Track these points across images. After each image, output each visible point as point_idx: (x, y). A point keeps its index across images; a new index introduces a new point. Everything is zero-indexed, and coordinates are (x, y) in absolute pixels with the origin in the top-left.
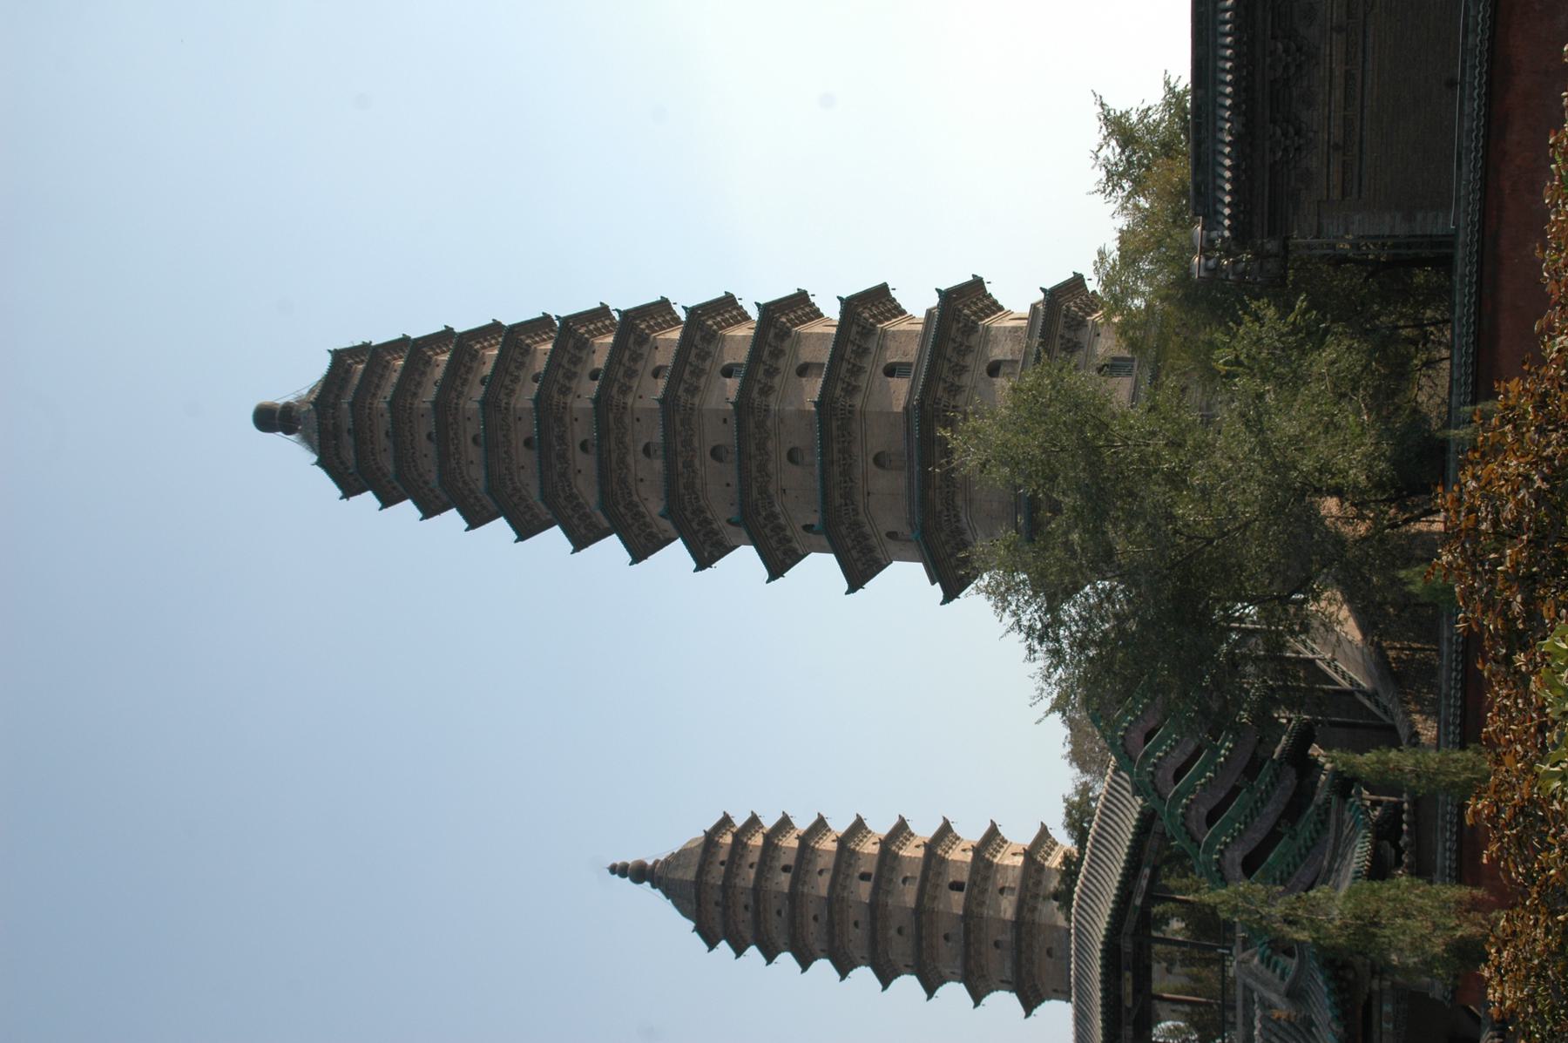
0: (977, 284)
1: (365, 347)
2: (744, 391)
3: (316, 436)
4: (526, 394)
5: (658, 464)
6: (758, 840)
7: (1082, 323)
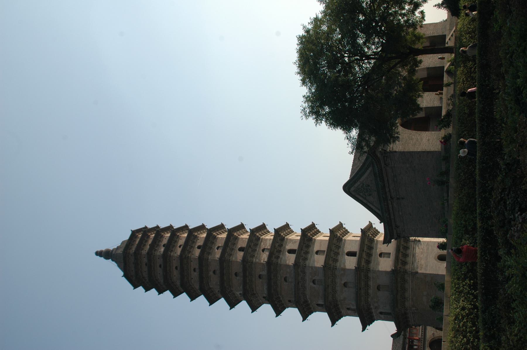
2: (270, 257)
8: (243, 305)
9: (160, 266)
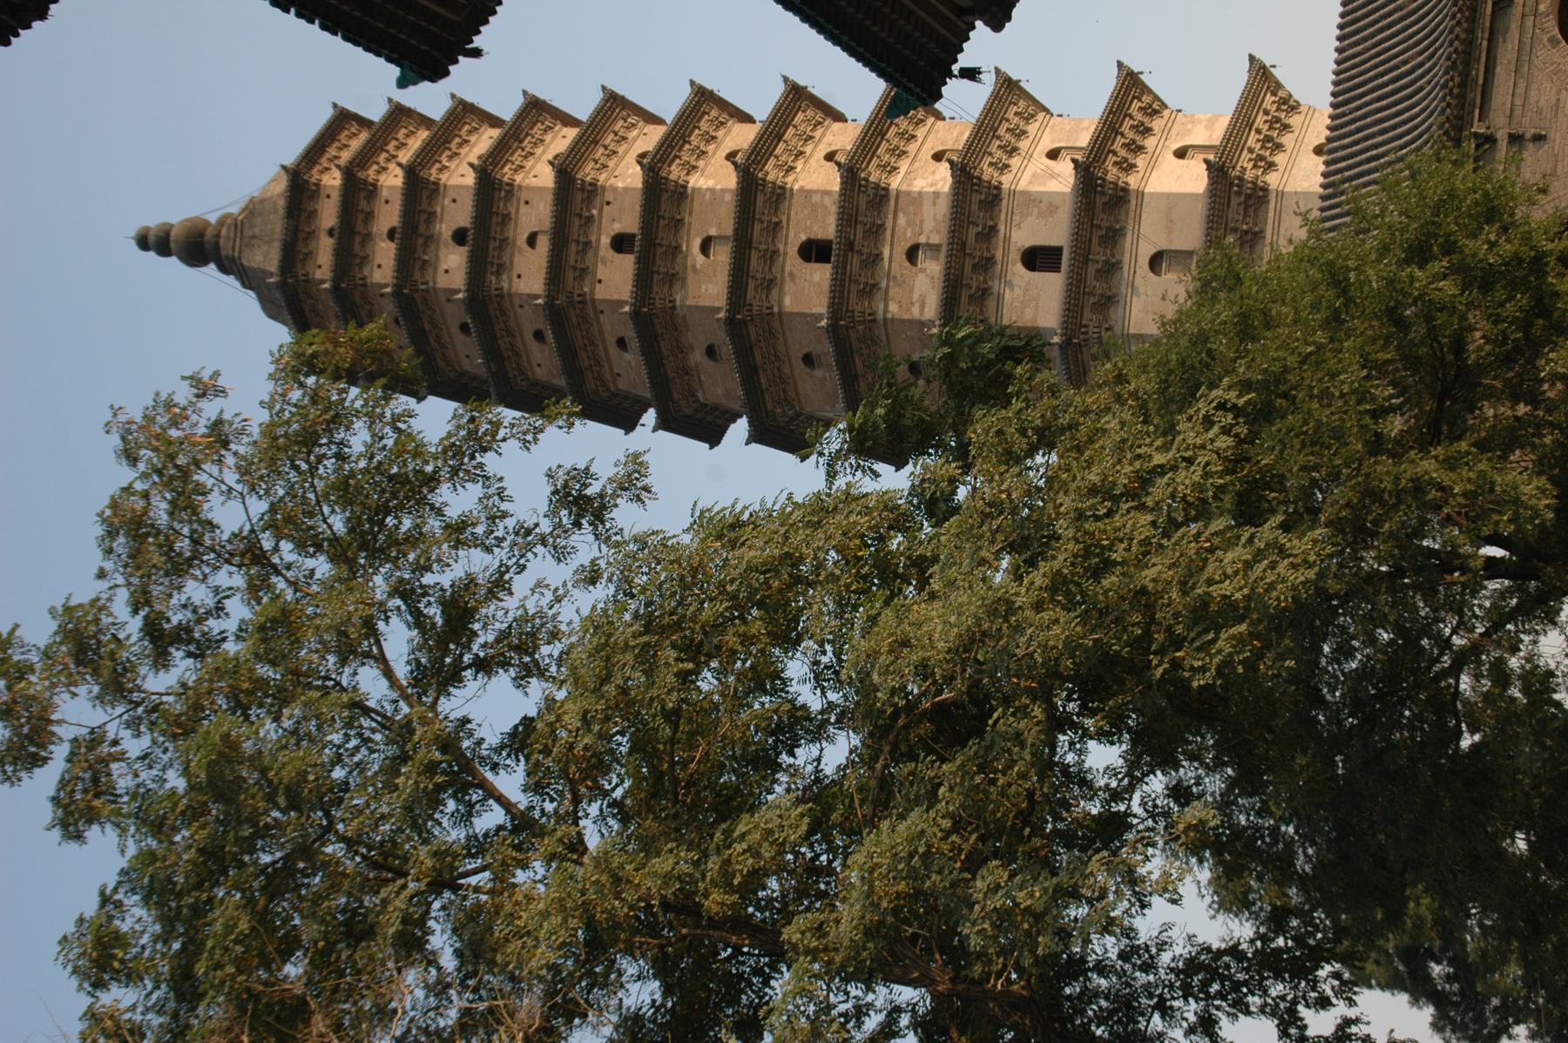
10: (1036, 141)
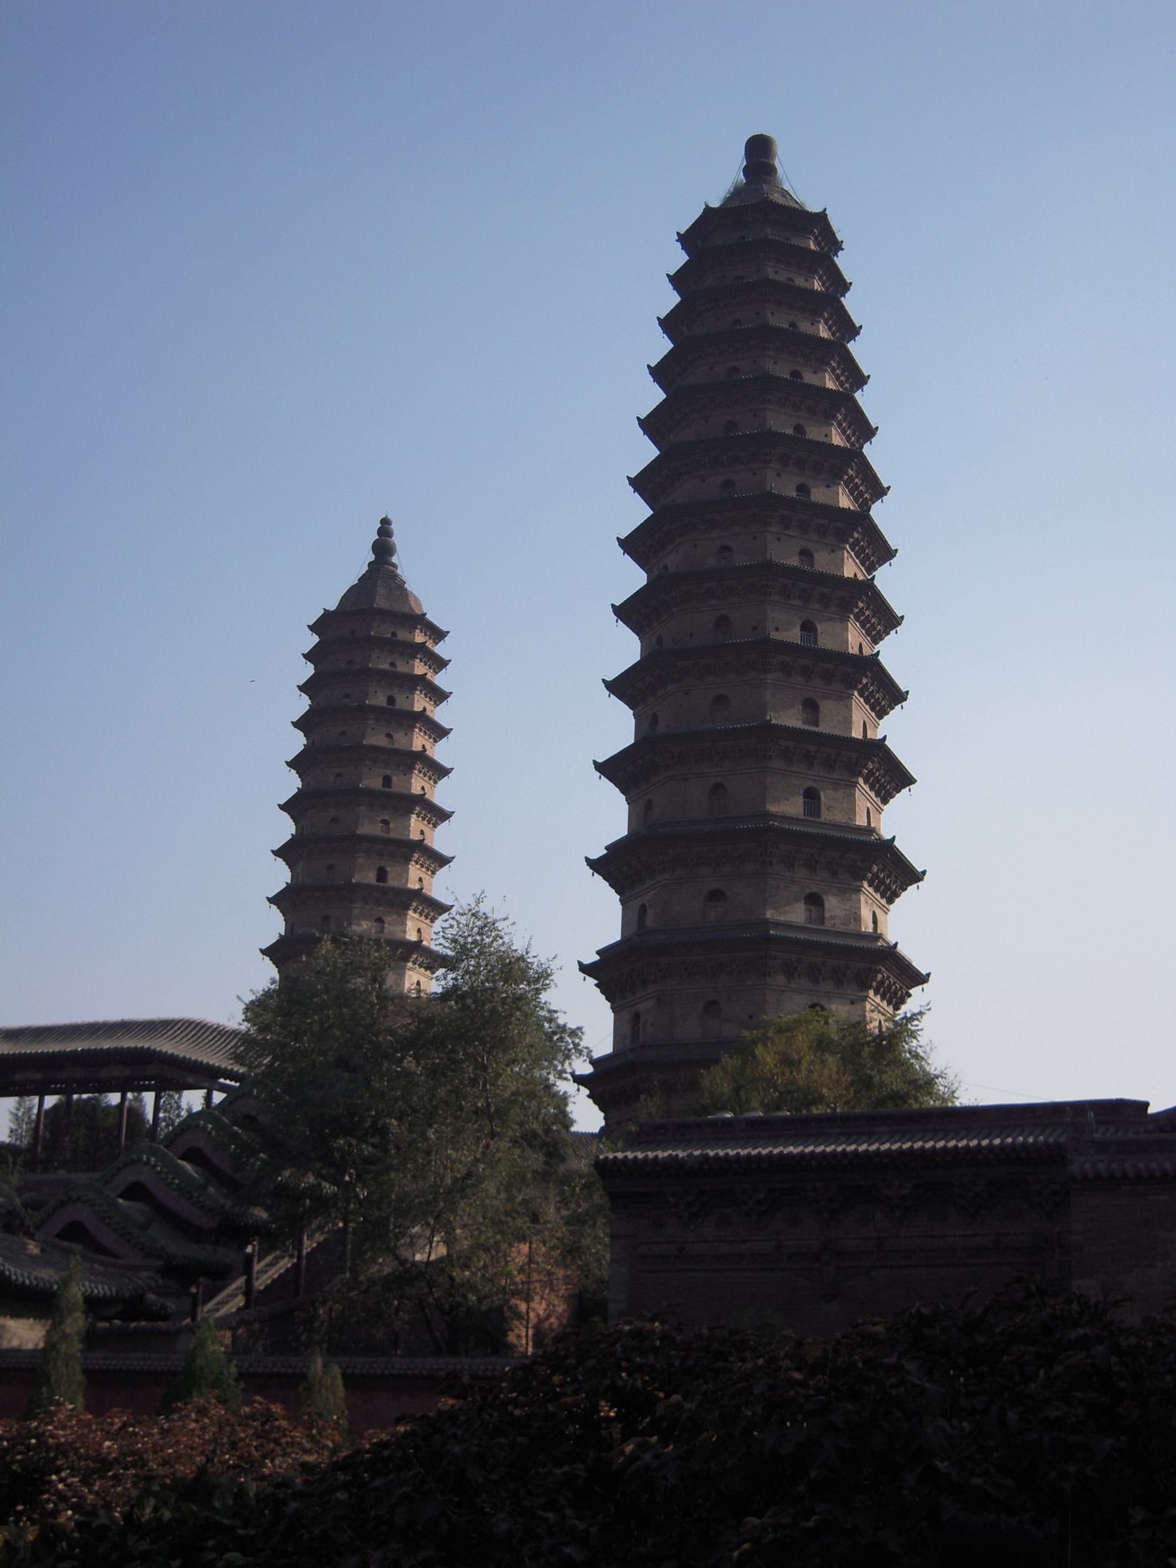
0: (911, 876)
1: (837, 246)
3: (737, 203)
4: (781, 423)
5: (711, 562)
6: (419, 668)
7: (865, 986)
8: (633, 578)
9: (737, 322)
10: (424, 975)
